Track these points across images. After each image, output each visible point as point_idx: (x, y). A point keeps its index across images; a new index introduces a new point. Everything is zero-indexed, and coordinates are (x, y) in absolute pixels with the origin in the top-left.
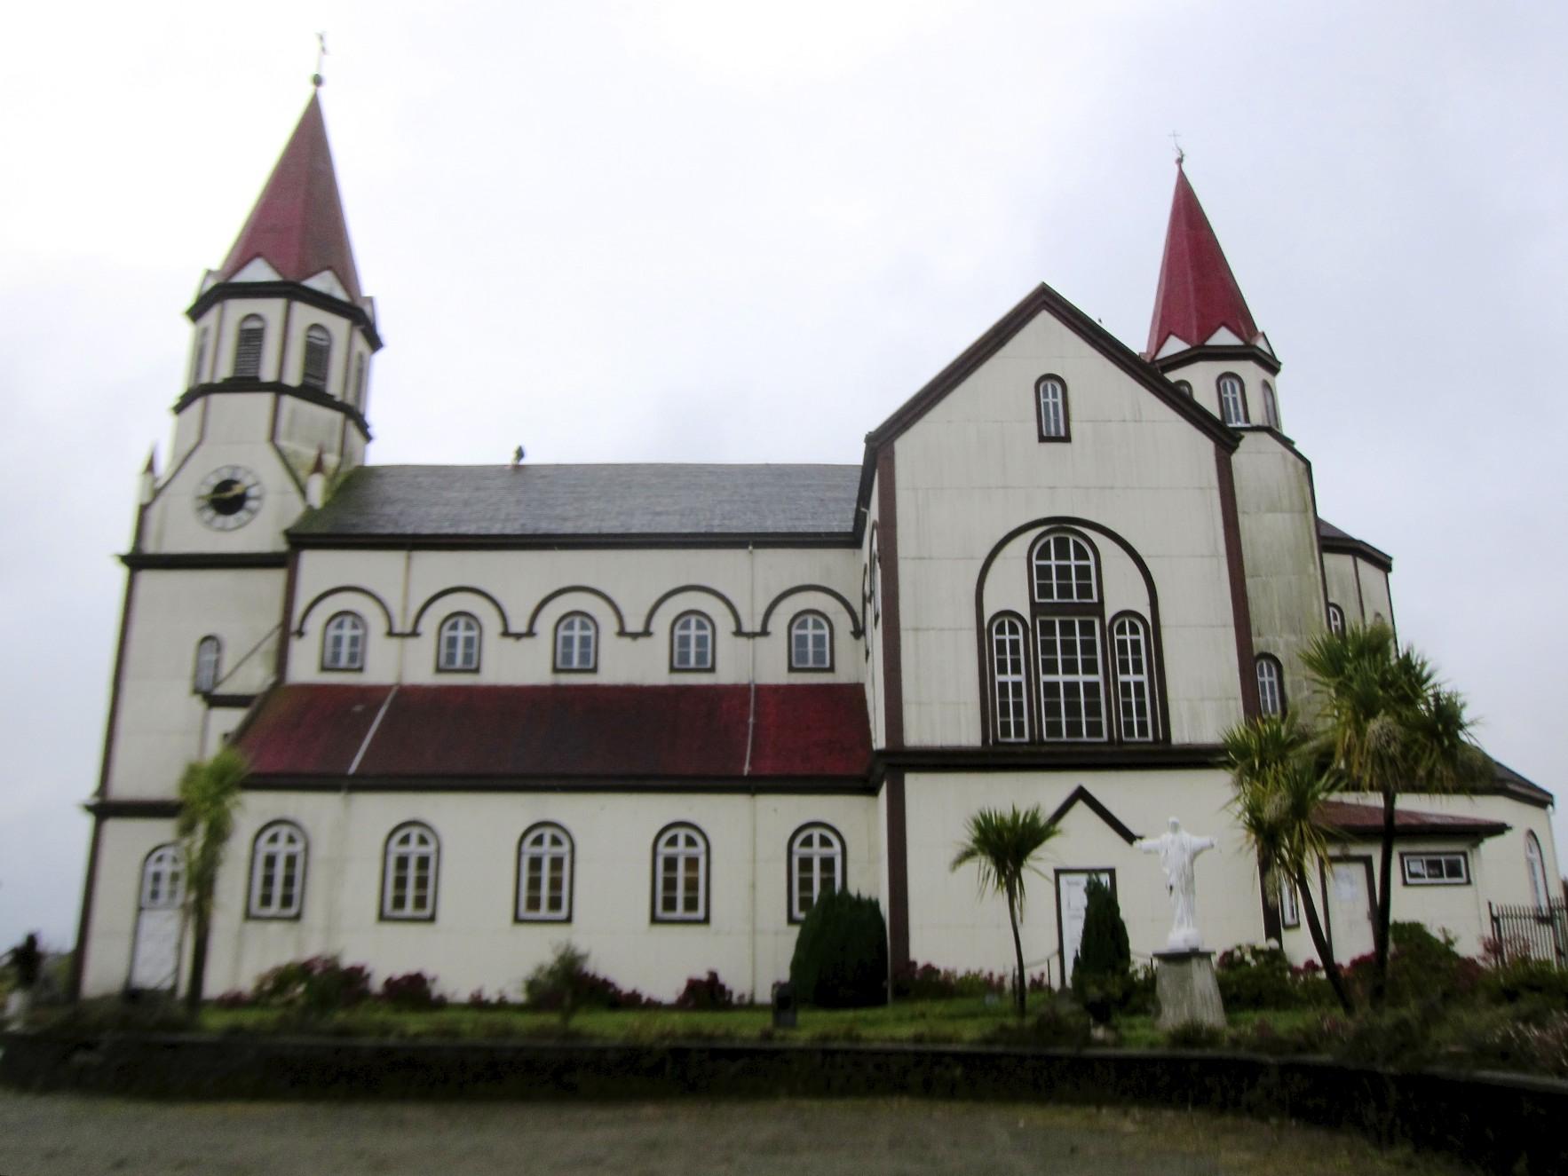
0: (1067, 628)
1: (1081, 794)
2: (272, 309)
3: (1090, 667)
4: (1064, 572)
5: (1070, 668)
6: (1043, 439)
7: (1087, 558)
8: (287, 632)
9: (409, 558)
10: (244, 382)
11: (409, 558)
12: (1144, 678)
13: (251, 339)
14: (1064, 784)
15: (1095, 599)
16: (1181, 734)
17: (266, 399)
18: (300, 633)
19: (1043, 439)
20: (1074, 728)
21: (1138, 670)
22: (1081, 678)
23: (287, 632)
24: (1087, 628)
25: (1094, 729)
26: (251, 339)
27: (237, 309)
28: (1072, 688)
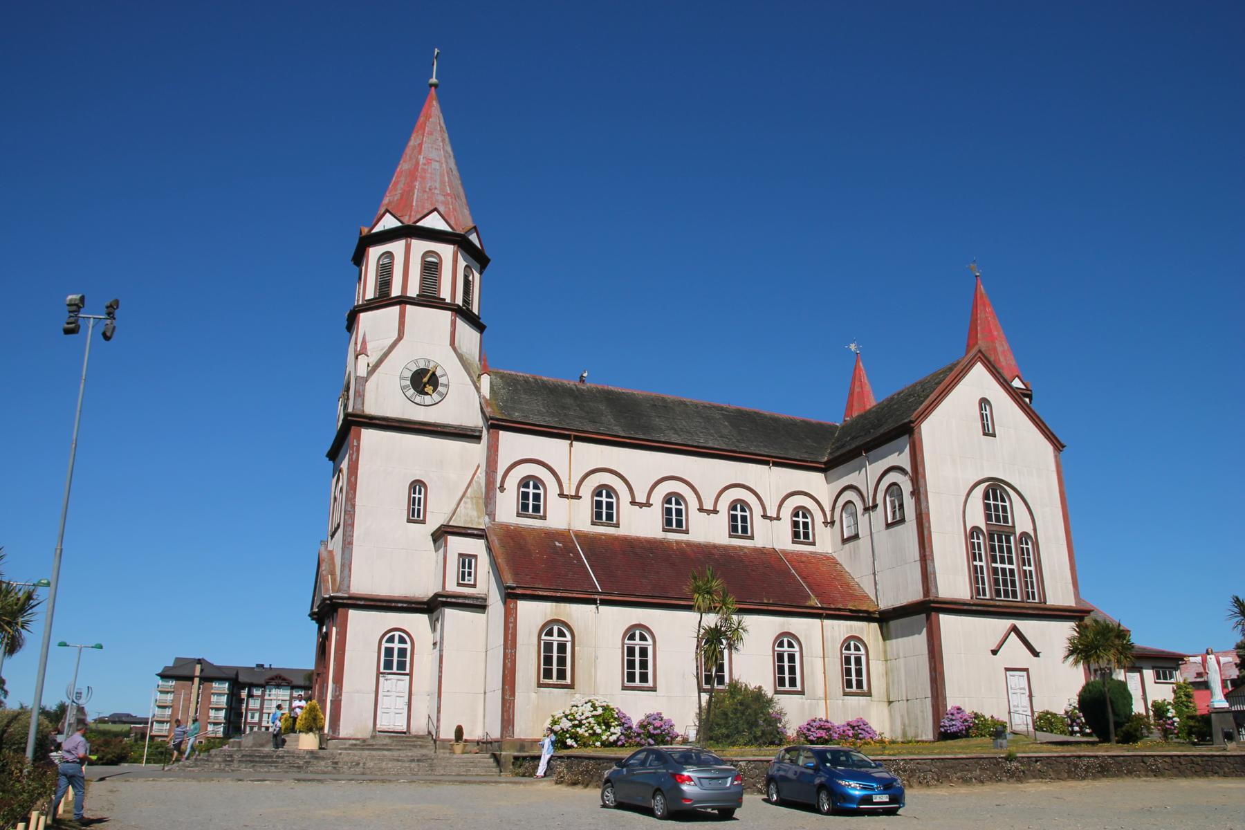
0: (1000, 540)
1: (1014, 629)
2: (446, 251)
3: (1011, 562)
4: (996, 507)
5: (1002, 562)
6: (985, 434)
7: (1005, 502)
8: (492, 487)
9: (571, 445)
10: (429, 299)
11: (571, 445)
12: (1032, 568)
13: (431, 269)
14: (1007, 623)
15: (1010, 524)
16: (1051, 601)
17: (447, 315)
18: (502, 489)
19: (984, 435)
20: (1006, 594)
21: (1030, 565)
22: (1007, 566)
23: (492, 487)
24: (1008, 541)
25: (1014, 594)
26: (431, 269)
27: (420, 247)
28: (1004, 570)
